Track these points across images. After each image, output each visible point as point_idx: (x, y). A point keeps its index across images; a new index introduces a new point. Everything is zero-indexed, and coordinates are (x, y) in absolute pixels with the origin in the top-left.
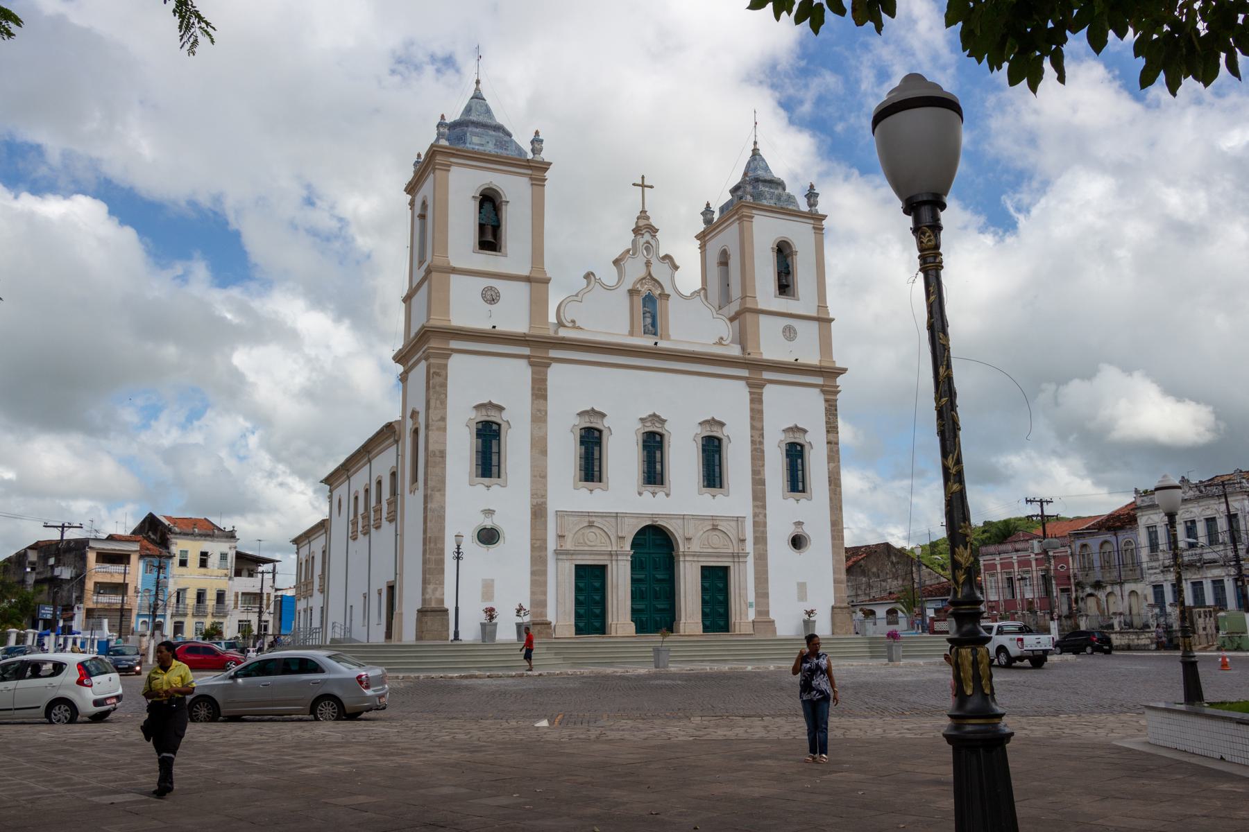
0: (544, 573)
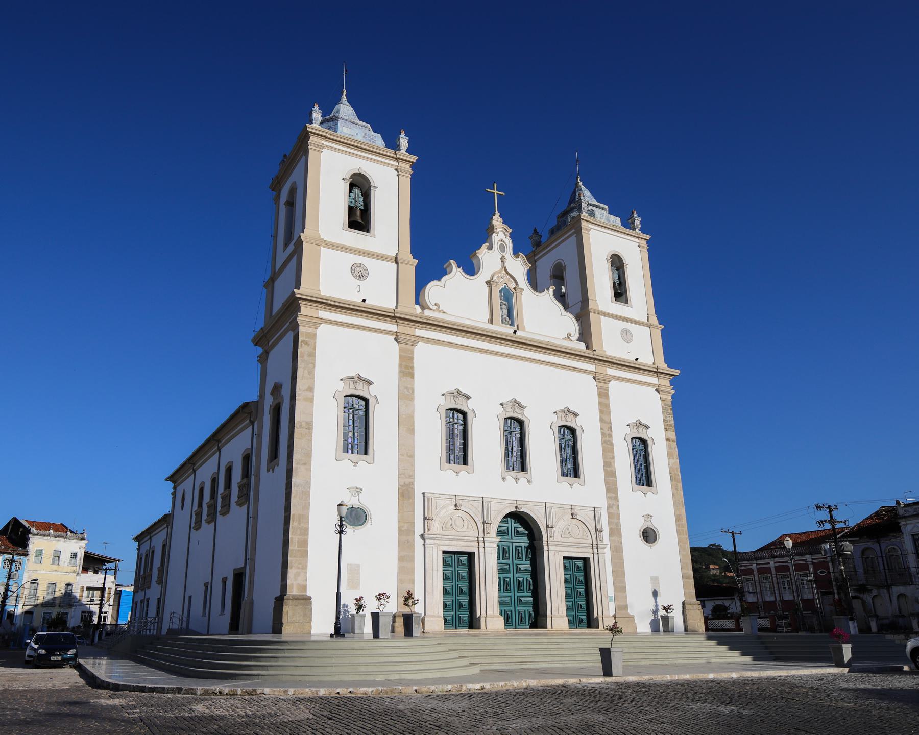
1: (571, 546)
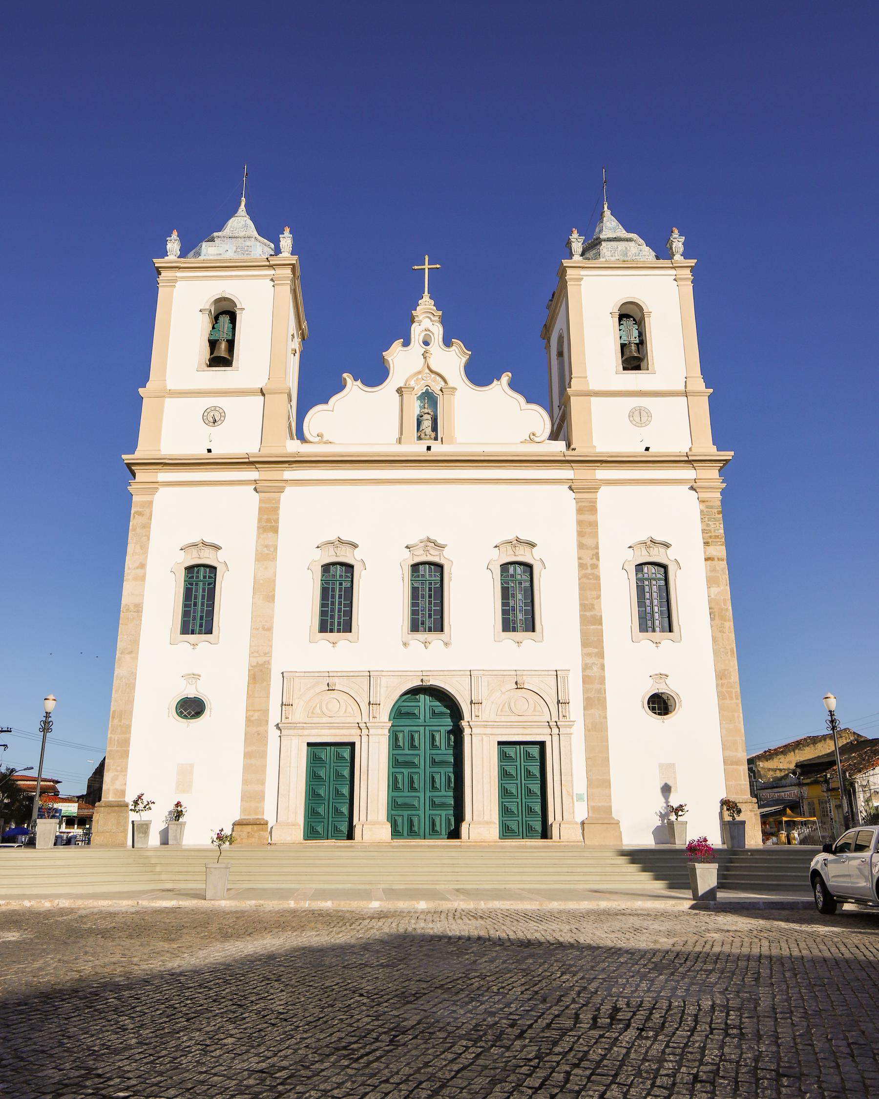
0: (263, 755)
1: (511, 727)
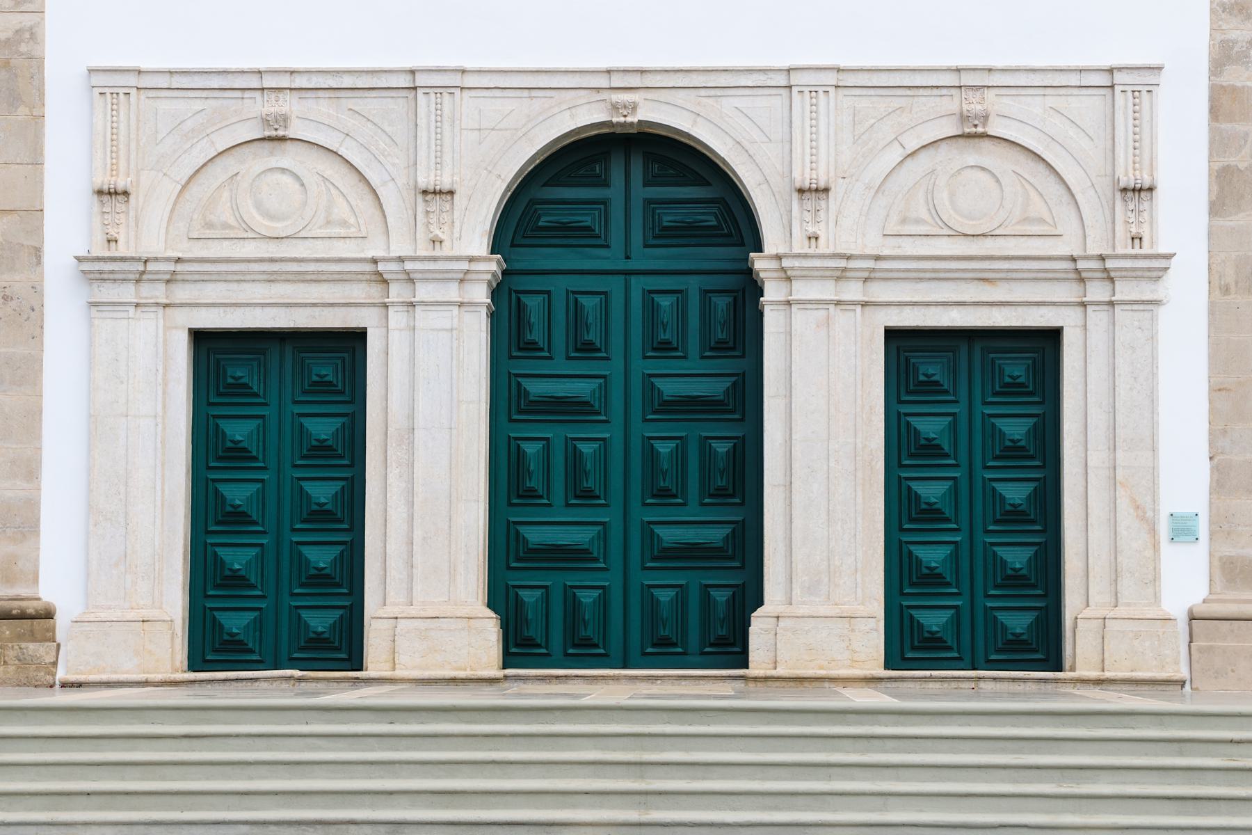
1: (938, 277)
